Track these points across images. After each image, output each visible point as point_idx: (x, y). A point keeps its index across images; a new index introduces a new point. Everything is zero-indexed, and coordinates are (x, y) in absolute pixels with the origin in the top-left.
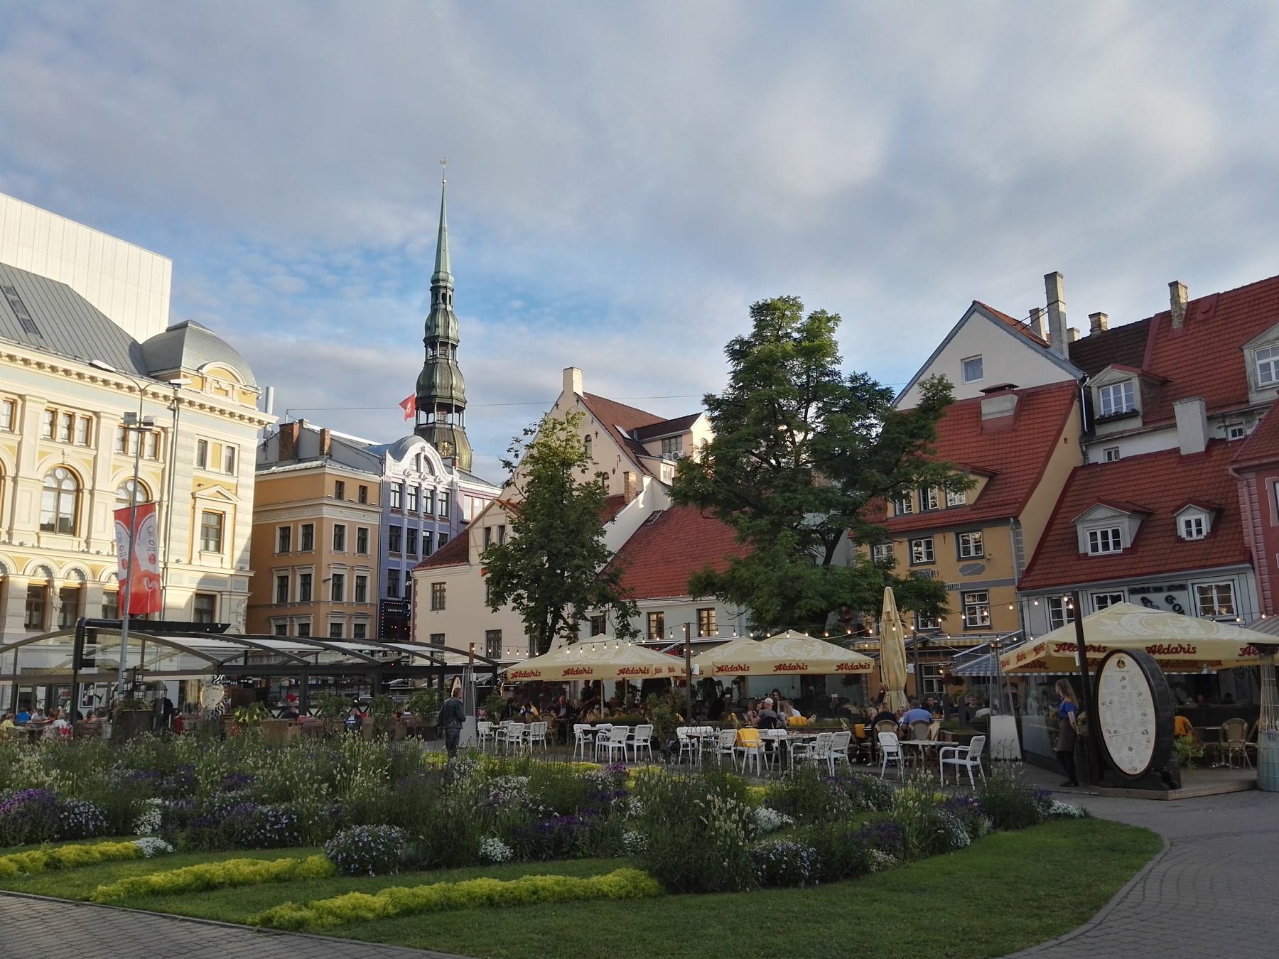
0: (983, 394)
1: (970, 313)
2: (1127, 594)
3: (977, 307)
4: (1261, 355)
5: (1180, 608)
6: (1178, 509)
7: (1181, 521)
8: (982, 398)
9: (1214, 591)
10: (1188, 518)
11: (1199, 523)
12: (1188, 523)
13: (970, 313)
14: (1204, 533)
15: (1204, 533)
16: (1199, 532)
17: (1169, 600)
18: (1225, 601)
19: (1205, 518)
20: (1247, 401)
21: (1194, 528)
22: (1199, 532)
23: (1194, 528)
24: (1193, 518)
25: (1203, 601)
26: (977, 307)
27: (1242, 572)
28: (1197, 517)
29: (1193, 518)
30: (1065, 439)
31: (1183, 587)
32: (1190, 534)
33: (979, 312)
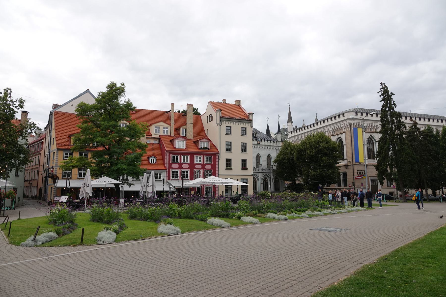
1: (86, 92)
3: (88, 91)
4: (156, 127)
6: (151, 156)
7: (151, 159)
9: (158, 174)
10: (152, 159)
11: (154, 160)
12: (152, 160)
13: (86, 92)
14: (155, 162)
15: (155, 162)
16: (154, 162)
18: (160, 176)
19: (155, 159)
20: (151, 136)
21: (153, 161)
22: (154, 162)
23: (153, 161)
24: (153, 159)
25: (161, 176)
26: (88, 91)
27: (164, 171)
28: (154, 159)
29: (153, 159)
32: (152, 162)
33: (89, 93)
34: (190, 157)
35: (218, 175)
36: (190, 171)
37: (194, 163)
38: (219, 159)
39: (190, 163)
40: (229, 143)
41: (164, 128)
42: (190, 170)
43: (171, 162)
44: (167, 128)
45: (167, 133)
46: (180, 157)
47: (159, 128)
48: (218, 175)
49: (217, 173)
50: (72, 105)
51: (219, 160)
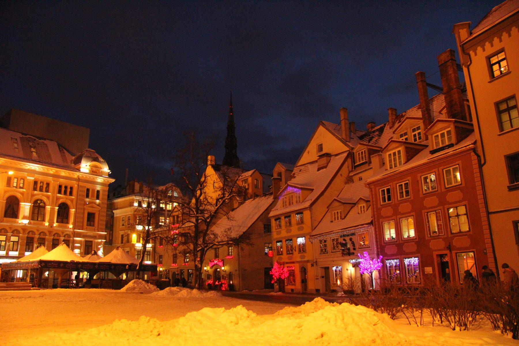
0: (318, 157)
2: (340, 238)
5: (354, 243)
8: (318, 159)
11: (364, 206)
17: (351, 239)
29: (362, 205)
30: (341, 174)
31: (353, 234)
34: (410, 181)
35: (489, 213)
36: (415, 216)
37: (421, 196)
38: (483, 162)
39: (412, 198)
40: (512, 103)
41: (414, 130)
42: (413, 213)
43: (379, 206)
44: (418, 128)
45: (420, 138)
46: (393, 188)
47: (406, 134)
48: (489, 213)
49: (482, 206)
50: (308, 152)
51: (481, 166)
